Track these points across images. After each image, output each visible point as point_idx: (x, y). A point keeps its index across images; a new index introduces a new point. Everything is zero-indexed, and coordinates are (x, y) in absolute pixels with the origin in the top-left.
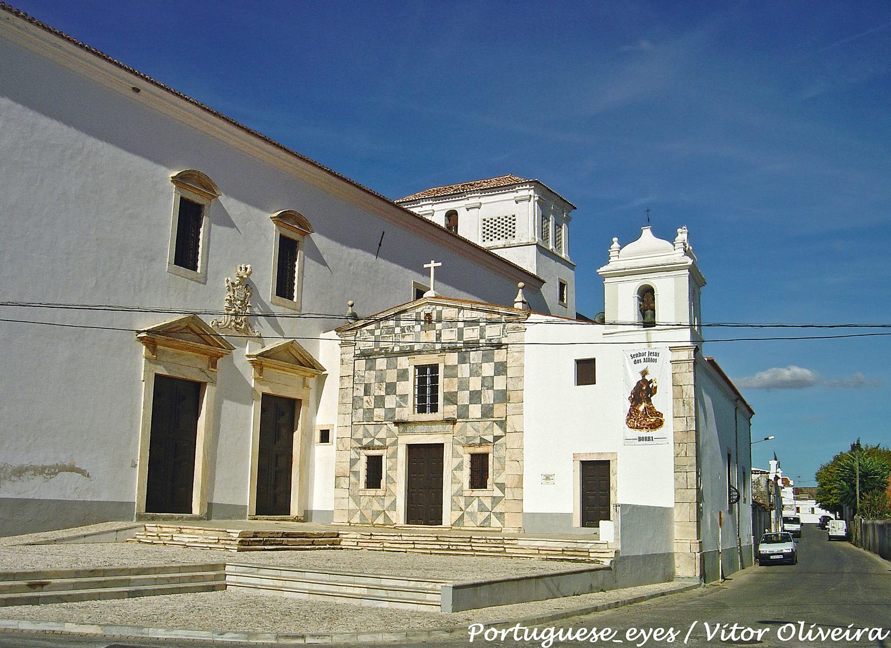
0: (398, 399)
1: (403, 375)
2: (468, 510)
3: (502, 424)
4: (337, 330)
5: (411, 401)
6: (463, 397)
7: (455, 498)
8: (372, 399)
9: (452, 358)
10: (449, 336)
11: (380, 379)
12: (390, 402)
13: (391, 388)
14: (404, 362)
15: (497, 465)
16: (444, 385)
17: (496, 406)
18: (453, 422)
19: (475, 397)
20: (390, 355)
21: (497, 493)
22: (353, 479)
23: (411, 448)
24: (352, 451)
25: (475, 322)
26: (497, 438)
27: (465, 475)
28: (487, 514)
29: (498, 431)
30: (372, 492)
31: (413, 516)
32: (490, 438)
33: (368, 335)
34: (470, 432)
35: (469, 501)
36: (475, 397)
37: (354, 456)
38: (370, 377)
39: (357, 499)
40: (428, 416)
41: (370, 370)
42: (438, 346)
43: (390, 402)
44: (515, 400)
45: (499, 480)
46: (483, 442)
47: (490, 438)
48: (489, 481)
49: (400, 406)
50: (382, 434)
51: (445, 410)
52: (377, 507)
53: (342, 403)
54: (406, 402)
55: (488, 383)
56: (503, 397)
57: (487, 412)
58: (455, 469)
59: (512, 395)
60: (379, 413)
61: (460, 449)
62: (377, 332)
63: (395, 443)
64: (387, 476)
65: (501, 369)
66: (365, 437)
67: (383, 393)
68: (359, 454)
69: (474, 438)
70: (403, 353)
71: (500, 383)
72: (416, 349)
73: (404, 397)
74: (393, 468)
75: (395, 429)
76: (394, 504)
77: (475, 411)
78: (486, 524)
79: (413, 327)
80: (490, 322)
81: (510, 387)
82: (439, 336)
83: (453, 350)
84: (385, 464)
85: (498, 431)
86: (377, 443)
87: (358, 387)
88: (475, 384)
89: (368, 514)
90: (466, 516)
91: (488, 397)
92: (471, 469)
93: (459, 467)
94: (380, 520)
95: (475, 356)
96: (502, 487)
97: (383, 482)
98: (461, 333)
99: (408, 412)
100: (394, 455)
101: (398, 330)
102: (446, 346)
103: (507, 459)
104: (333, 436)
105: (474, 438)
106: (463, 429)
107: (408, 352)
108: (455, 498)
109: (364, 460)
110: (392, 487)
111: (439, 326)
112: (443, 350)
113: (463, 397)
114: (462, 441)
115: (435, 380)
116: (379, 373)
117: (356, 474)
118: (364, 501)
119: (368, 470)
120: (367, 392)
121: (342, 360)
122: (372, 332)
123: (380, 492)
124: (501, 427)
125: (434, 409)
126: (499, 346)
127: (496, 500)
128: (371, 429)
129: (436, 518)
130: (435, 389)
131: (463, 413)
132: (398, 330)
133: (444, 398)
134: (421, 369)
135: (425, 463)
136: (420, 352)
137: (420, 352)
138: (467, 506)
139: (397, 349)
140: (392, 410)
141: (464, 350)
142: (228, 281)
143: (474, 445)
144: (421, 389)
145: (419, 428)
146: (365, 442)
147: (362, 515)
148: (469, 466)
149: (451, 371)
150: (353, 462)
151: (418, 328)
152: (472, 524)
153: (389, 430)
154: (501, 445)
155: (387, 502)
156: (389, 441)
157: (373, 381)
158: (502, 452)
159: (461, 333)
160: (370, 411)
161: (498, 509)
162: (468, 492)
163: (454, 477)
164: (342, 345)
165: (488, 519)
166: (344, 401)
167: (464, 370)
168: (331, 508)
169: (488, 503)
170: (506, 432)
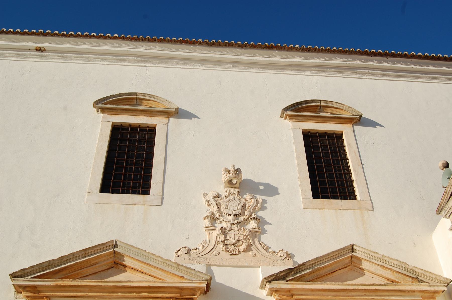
4: (439, 211)
142: (205, 195)
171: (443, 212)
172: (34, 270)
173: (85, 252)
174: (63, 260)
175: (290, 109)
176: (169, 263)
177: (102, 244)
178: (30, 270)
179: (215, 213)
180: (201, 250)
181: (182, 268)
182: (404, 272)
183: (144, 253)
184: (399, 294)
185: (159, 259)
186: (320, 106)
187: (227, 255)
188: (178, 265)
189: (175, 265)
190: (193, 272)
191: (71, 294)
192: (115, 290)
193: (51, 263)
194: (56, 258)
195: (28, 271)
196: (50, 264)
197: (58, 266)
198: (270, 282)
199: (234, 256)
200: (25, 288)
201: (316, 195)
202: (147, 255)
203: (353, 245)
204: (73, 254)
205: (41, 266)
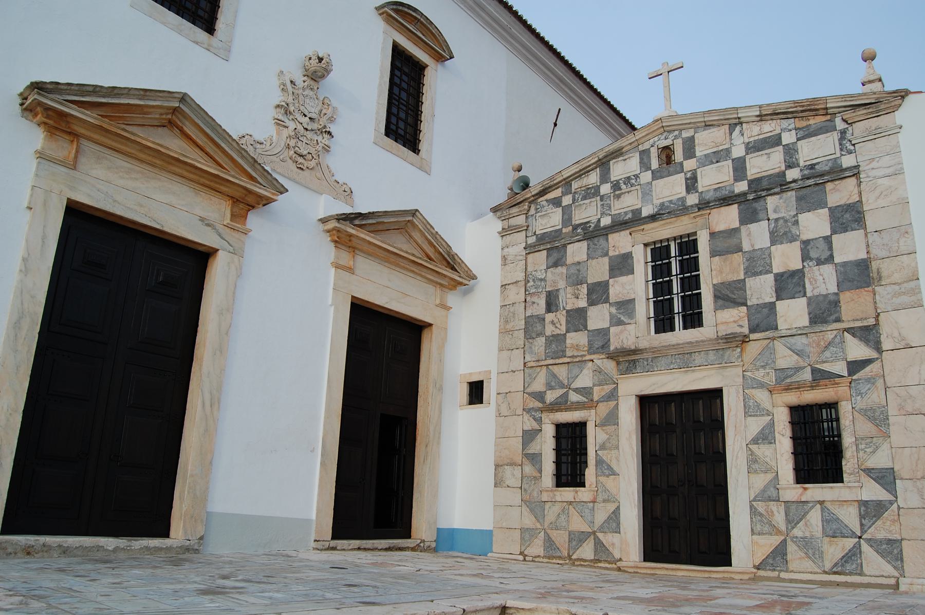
0: (613, 310)
1: (622, 265)
2: (797, 532)
3: (868, 333)
5: (644, 309)
6: (761, 289)
7: (761, 507)
8: (561, 317)
9: (728, 217)
10: (714, 178)
11: (576, 280)
12: (598, 317)
13: (598, 294)
14: (620, 242)
15: (865, 427)
16: (711, 272)
17: (845, 297)
18: (744, 340)
19: (789, 284)
20: (593, 234)
21: (873, 492)
22: (528, 469)
23: (645, 402)
24: (526, 416)
25: (775, 141)
26: (855, 366)
27: (782, 453)
28: (850, 543)
29: (857, 350)
30: (568, 493)
31: (661, 544)
32: (840, 368)
33: (550, 209)
34: (785, 358)
35: (796, 512)
36: (789, 284)
37: (530, 424)
38: (557, 278)
39: (536, 507)
40: (680, 335)
41: (556, 265)
42: (692, 200)
43: (598, 317)
44: (897, 277)
45: (880, 460)
46: (821, 377)
47: (840, 368)
48: (848, 465)
49: (620, 323)
50: (585, 379)
51: (718, 319)
52: (578, 524)
53: (505, 332)
54: (631, 314)
55: (817, 252)
56: (860, 275)
57: (824, 312)
58: (755, 441)
59: (885, 267)
60: (576, 339)
61: (761, 396)
62: (567, 200)
63: (613, 396)
64: (599, 462)
65: (850, 217)
66: (551, 388)
67: (582, 303)
68: (539, 421)
69: (798, 369)
70: (620, 225)
71: (849, 248)
72: (645, 213)
73: (626, 306)
74: (609, 445)
75: (610, 366)
76: (614, 522)
77: (793, 313)
78: (849, 567)
79: (637, 176)
80: (807, 134)
81: (875, 251)
82: (691, 184)
83: (726, 200)
84: (594, 437)
85: (857, 350)
86: (574, 397)
87: (535, 299)
88: (787, 257)
89: (561, 538)
90: (791, 548)
91: (823, 281)
92: (794, 438)
93: (766, 436)
94: (587, 551)
95: (777, 205)
96: (886, 478)
97: (590, 474)
98: (739, 168)
99: (639, 331)
100: (612, 419)
101: (605, 189)
102: (710, 196)
103: (892, 411)
104: (490, 392)
105: (798, 369)
106: (768, 355)
107: (630, 222)
108: (761, 507)
109: (549, 431)
110: (609, 482)
111: (690, 165)
112: (704, 205)
113: (761, 289)
114: (766, 380)
115: (690, 265)
116: (573, 270)
117: (535, 459)
118: (552, 513)
119: (558, 451)
120: (551, 304)
121: (504, 258)
122: (557, 202)
123: (583, 494)
124: (866, 341)
125: (693, 319)
126: (837, 173)
127: (871, 511)
128: (562, 372)
129: (714, 549)
130: (691, 283)
131: (764, 320)
132: (605, 189)
133: (716, 297)
134: (659, 252)
135: (683, 435)
136: (653, 218)
137: (653, 218)
138: (792, 522)
139: (606, 221)
140: (604, 333)
141: (751, 197)
143: (799, 387)
144: (661, 289)
145: (663, 362)
146: (551, 397)
147: (549, 543)
148: (788, 433)
149: (726, 243)
150: (529, 436)
151: (646, 177)
152: (808, 565)
153: (598, 371)
154: (871, 380)
155: (601, 516)
156: (597, 394)
157: (561, 284)
158: (875, 397)
159: (739, 168)
160: (559, 339)
161: (881, 530)
162: (791, 491)
163: (753, 460)
164: (504, 233)
165: (853, 555)
166: (509, 327)
167: (757, 235)
168: (486, 524)
169: (850, 517)
170: (878, 348)
171: (499, 214)
172: (70, 90)
173: (145, 93)
174: (113, 91)
175: (391, 7)
176: (245, 154)
177: (169, 92)
178: (65, 87)
179: (291, 105)
180: (268, 148)
181: (258, 167)
182: (446, 256)
183: (218, 128)
184: (435, 274)
185: (234, 144)
186: (419, 20)
187: (293, 167)
188: (255, 161)
189: (251, 160)
190: (269, 177)
191: (119, 146)
192: (173, 161)
193: (98, 89)
194: (106, 85)
195: (62, 87)
196: (96, 90)
197: (104, 97)
198: (338, 220)
199: (300, 171)
200: (48, 109)
201: (388, 133)
202: (221, 132)
203: (417, 210)
204: (130, 89)
205: (82, 89)
